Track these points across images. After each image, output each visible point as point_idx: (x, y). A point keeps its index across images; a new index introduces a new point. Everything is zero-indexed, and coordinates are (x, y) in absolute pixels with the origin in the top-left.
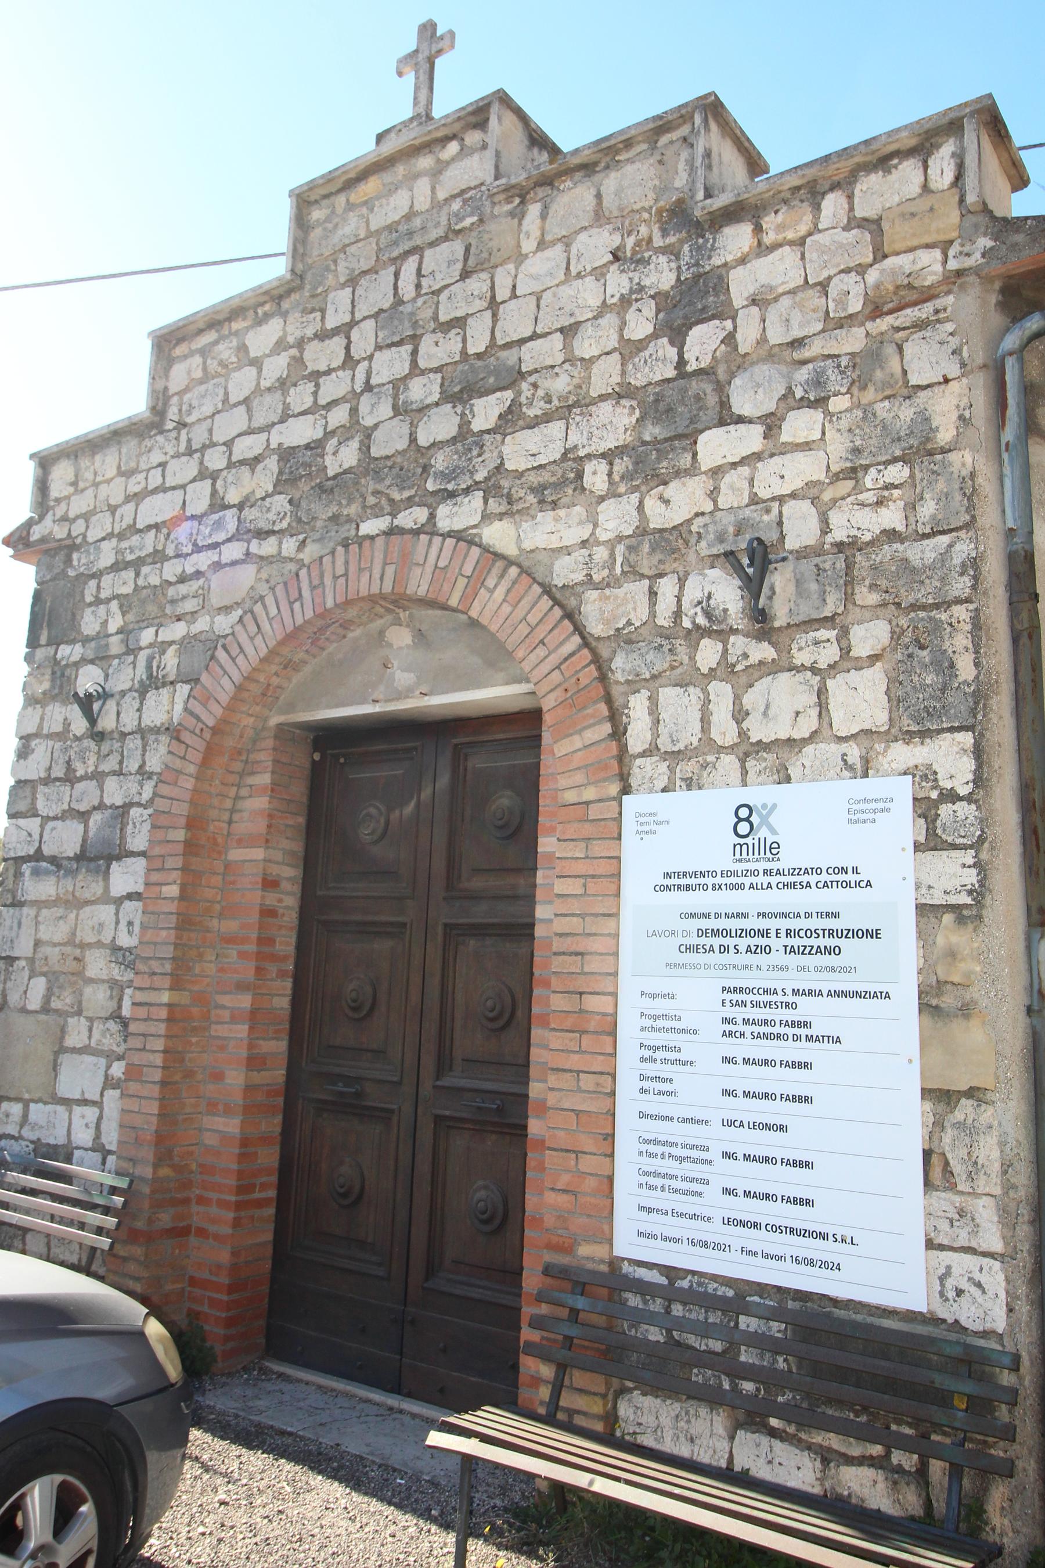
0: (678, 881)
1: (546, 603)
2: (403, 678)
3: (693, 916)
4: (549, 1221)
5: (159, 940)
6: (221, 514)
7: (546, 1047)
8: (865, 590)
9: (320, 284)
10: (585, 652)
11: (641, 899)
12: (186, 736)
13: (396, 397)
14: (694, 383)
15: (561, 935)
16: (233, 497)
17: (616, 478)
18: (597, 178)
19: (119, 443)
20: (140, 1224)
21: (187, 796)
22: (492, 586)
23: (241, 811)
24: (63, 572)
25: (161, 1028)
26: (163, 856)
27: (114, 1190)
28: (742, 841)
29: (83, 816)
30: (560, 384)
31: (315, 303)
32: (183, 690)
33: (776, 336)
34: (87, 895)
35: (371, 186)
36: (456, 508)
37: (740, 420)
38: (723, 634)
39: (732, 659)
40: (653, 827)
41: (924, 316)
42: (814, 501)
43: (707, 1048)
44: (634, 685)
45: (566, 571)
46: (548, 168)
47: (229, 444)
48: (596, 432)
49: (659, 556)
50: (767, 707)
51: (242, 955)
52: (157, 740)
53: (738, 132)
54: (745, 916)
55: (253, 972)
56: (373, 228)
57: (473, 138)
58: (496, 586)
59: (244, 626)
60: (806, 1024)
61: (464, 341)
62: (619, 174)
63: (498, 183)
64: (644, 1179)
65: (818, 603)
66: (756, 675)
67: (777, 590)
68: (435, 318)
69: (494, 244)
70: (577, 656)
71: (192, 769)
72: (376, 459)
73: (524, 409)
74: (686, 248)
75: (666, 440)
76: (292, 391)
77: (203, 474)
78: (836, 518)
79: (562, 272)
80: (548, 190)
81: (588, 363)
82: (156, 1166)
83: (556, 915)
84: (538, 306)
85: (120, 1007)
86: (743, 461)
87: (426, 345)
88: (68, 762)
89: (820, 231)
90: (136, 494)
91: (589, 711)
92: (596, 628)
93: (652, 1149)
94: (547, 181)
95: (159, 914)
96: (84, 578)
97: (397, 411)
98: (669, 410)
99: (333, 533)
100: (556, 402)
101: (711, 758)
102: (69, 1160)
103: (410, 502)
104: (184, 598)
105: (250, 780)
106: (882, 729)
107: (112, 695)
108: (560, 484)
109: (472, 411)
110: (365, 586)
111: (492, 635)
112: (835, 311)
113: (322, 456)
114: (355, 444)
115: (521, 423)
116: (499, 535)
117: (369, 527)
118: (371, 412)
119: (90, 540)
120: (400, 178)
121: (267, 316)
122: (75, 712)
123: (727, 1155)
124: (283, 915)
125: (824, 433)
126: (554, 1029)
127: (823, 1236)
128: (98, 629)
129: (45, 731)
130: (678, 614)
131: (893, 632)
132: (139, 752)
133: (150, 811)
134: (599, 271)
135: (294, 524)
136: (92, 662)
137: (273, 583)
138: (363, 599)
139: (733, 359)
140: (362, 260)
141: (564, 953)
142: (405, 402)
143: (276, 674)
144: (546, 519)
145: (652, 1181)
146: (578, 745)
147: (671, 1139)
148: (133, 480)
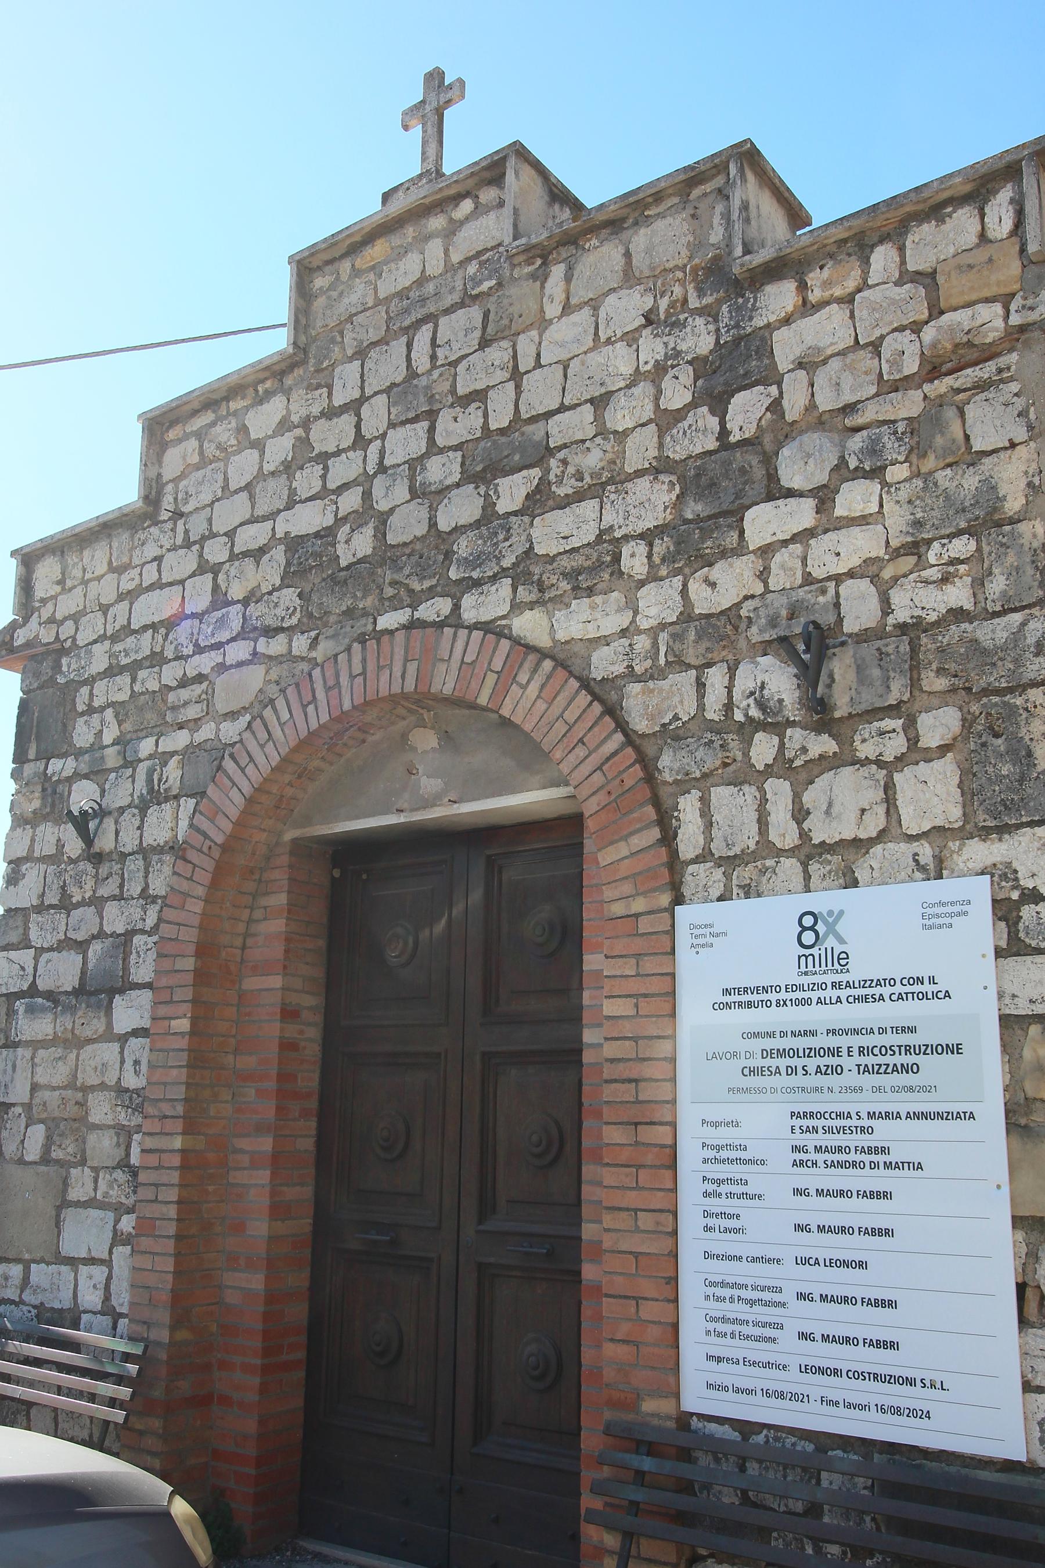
0: (739, 997)
1: (584, 698)
2: (429, 785)
3: (756, 1035)
4: (609, 1374)
5: (169, 1080)
6: (224, 610)
7: (599, 1184)
8: (932, 674)
9: (325, 357)
10: (629, 750)
11: (700, 1020)
12: (192, 855)
13: (412, 479)
14: (738, 455)
15: (612, 1061)
16: (237, 592)
17: (657, 559)
18: (625, 235)
19: (109, 536)
20: (158, 1393)
21: (196, 921)
22: (524, 682)
23: (254, 935)
24: (52, 680)
25: (175, 1177)
26: (171, 987)
27: (127, 1357)
28: (807, 952)
29: (82, 946)
30: (593, 460)
31: (321, 379)
32: (188, 804)
33: (826, 401)
34: (88, 1032)
35: (378, 250)
36: (483, 597)
37: (790, 493)
38: (778, 728)
39: (789, 754)
40: (710, 940)
41: (986, 376)
42: (874, 579)
43: (775, 1180)
44: (683, 786)
45: (605, 663)
46: (576, 228)
47: (231, 534)
48: (633, 511)
49: (705, 644)
50: (830, 805)
51: (260, 1093)
52: (160, 860)
53: (777, 181)
54: (813, 1033)
55: (273, 1112)
56: (382, 295)
57: (488, 195)
58: (528, 682)
59: (253, 733)
60: (884, 1150)
61: (486, 416)
62: (649, 231)
63: (517, 243)
64: (711, 1326)
65: (881, 690)
66: (815, 772)
67: (837, 677)
68: (453, 391)
69: (515, 310)
70: (620, 755)
71: (200, 891)
72: (393, 546)
73: (554, 488)
74: (725, 308)
75: (710, 517)
76: (298, 475)
77: (203, 568)
78: (898, 597)
79: (591, 337)
80: (572, 249)
81: (621, 436)
82: (173, 1328)
83: (606, 1039)
84: (565, 376)
85: (128, 1155)
86: (794, 538)
87: (444, 420)
88: (63, 887)
89: (870, 287)
90: (129, 592)
91: (634, 815)
92: (640, 725)
93: (720, 1292)
94: (572, 240)
95: (167, 1051)
96: (72, 686)
97: (414, 494)
98: (712, 484)
99: (348, 629)
100: (588, 479)
101: (770, 863)
102: (76, 1326)
103: (431, 593)
104: (186, 704)
105: (264, 901)
106: (956, 826)
107: (110, 813)
108: (596, 569)
109: (496, 491)
110: (384, 685)
111: (527, 735)
112: (890, 373)
113: (334, 545)
114: (369, 531)
115: (551, 503)
116: (530, 625)
117: (388, 621)
118: (387, 495)
119: (80, 643)
120: (410, 240)
121: (269, 394)
122: (69, 832)
123: (802, 1296)
124: (305, 1048)
125: (881, 506)
126: (608, 1164)
127: (910, 1382)
128: (91, 740)
129: (37, 854)
130: (729, 707)
131: (964, 720)
132: (141, 874)
133: (155, 938)
134: (630, 336)
135: (305, 620)
136: (86, 776)
137: (283, 684)
138: (383, 699)
139: (780, 429)
140: (371, 330)
141: (616, 1081)
142: (422, 484)
143: (290, 784)
144: (581, 606)
146: (625, 852)
147: (741, 1281)
148: (125, 577)
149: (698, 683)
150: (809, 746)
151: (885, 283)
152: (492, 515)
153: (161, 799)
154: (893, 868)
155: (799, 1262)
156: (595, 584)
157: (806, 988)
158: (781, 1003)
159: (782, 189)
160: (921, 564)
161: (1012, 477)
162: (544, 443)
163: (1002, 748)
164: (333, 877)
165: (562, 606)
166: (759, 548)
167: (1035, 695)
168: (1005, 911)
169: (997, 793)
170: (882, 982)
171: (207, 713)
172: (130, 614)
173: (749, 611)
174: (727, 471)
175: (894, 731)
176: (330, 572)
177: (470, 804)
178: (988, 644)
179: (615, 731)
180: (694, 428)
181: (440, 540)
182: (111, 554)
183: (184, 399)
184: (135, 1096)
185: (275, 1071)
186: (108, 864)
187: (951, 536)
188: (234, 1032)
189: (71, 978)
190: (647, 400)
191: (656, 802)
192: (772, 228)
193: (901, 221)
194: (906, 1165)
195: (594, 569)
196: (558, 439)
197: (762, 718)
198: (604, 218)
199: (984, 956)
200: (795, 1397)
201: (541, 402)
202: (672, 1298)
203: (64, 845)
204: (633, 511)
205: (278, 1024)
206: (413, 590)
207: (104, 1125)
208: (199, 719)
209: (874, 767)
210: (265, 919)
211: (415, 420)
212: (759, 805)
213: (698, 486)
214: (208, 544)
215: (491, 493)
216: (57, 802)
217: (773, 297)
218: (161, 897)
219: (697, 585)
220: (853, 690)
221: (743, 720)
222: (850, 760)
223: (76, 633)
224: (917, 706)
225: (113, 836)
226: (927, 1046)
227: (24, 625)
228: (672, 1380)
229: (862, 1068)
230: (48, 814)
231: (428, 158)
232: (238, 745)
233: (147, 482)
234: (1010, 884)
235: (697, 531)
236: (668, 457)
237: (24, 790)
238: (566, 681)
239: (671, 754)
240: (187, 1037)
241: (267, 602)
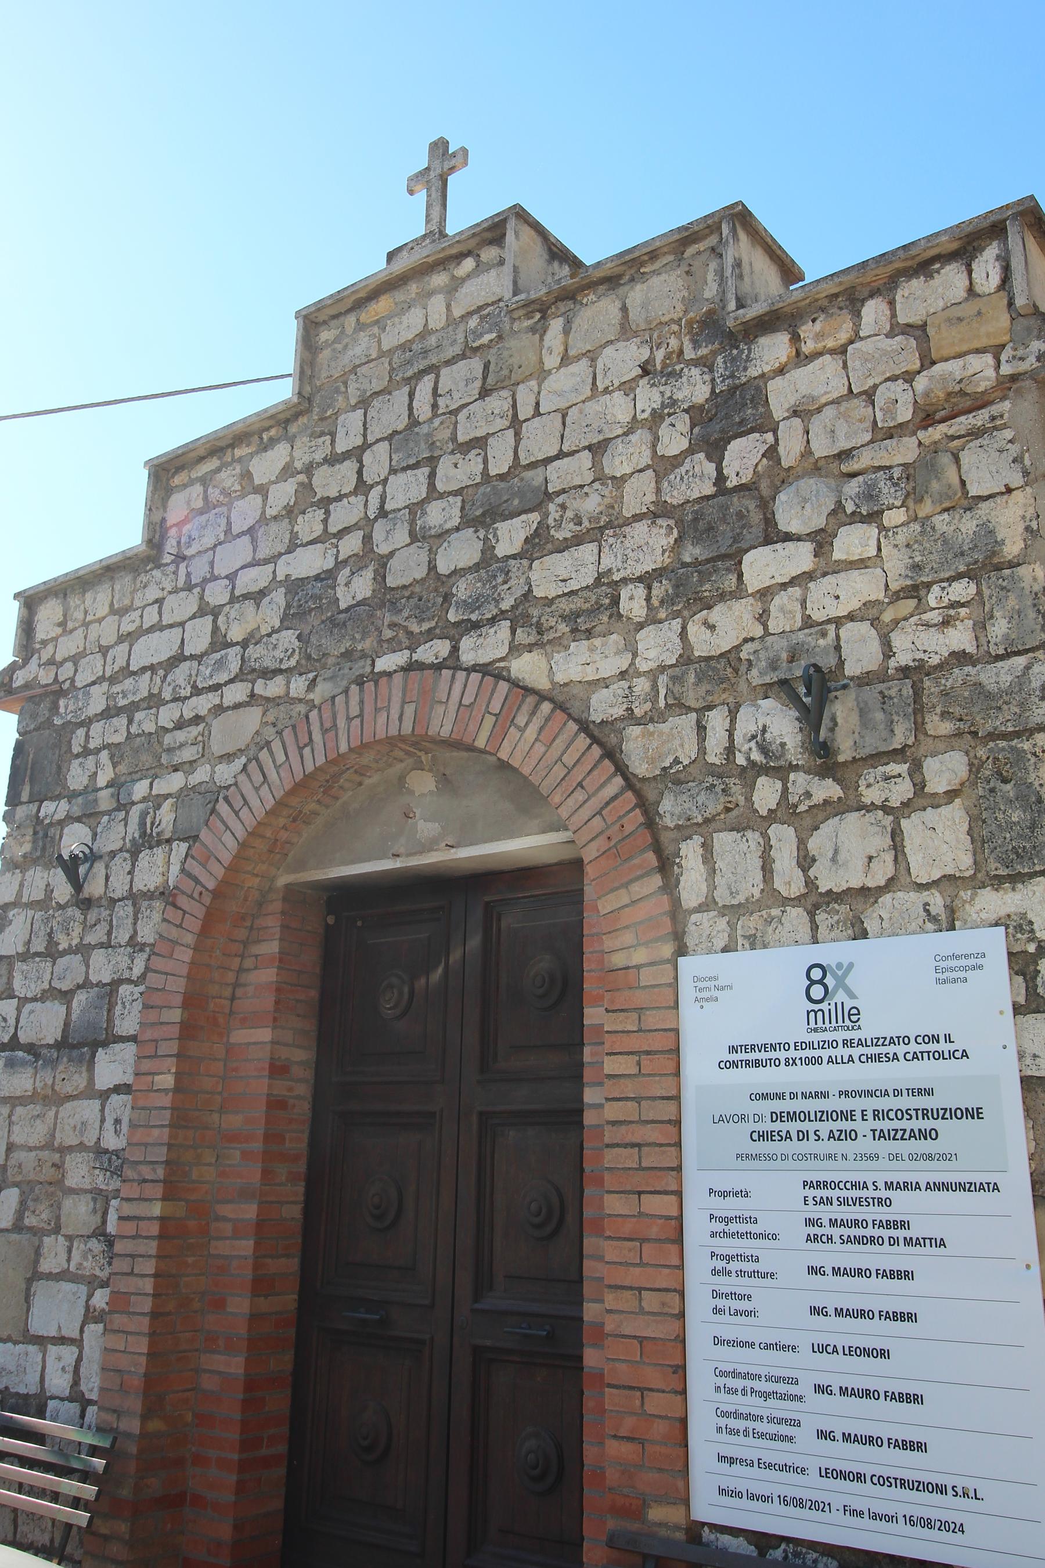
0: (745, 1056)
1: (583, 741)
2: (426, 829)
3: (765, 1096)
4: (612, 1476)
5: (150, 1140)
6: (223, 652)
7: (600, 1258)
8: (936, 718)
9: (329, 407)
10: (629, 794)
11: (703, 1073)
12: (183, 901)
13: (412, 522)
14: (735, 499)
15: (614, 1123)
16: (236, 634)
17: (655, 602)
18: (621, 291)
19: (112, 579)
20: (125, 1492)
21: (184, 971)
22: (522, 725)
23: (245, 985)
24: (49, 722)
25: (152, 1247)
26: (156, 1041)
27: (94, 1451)
28: (816, 1007)
29: (66, 996)
30: (591, 504)
31: (324, 427)
32: (180, 849)
33: (821, 448)
34: (68, 1089)
35: (383, 305)
36: (481, 640)
37: (788, 537)
38: (782, 772)
39: (793, 799)
40: (715, 993)
41: (980, 423)
42: (875, 622)
43: (789, 1256)
44: (685, 830)
45: (604, 706)
46: (572, 283)
47: (232, 577)
48: (631, 554)
49: (705, 687)
50: (836, 852)
51: (245, 1155)
52: (150, 907)
53: (769, 240)
54: (825, 1095)
55: (259, 1176)
56: (385, 347)
57: (489, 254)
58: (527, 724)
59: (249, 776)
60: (903, 1225)
61: (485, 462)
62: (645, 286)
63: (516, 298)
64: (723, 1422)
65: (885, 734)
66: (820, 817)
67: (839, 720)
68: (454, 438)
69: (515, 361)
70: (621, 799)
71: (189, 939)
72: (393, 589)
73: (552, 532)
74: (720, 359)
75: (708, 561)
76: (300, 519)
77: (204, 609)
78: (899, 641)
79: (589, 387)
80: (570, 304)
81: (619, 481)
82: (145, 1418)
83: (607, 1099)
84: (564, 424)
85: (104, 1222)
86: (793, 582)
87: (444, 467)
88: (50, 935)
89: (862, 339)
90: (129, 634)
91: (636, 861)
92: (640, 768)
93: (731, 1383)
94: (569, 296)
95: (150, 1109)
96: (70, 727)
97: (414, 537)
98: (710, 528)
99: (346, 671)
100: (586, 523)
101: (775, 912)
102: (41, 1414)
103: (430, 635)
104: (182, 745)
105: (256, 949)
106: (967, 874)
107: (101, 857)
108: (594, 611)
109: (495, 535)
110: (382, 727)
111: (525, 778)
112: (884, 421)
113: (334, 588)
114: (369, 574)
115: (549, 546)
116: (528, 667)
117: (386, 662)
118: (387, 539)
119: (79, 684)
120: (413, 296)
121: (273, 442)
122: (59, 878)
123: (820, 1389)
124: (294, 1106)
125: (879, 549)
126: (609, 1238)
127: (941, 1489)
128: (86, 782)
129: (24, 900)
130: (730, 750)
131: (971, 765)
132: (130, 920)
133: (142, 988)
134: (627, 386)
135: (303, 662)
136: (78, 820)
137: (280, 726)
138: (380, 741)
139: (776, 474)
140: (374, 381)
141: (618, 1145)
142: (423, 528)
143: (285, 828)
144: (580, 649)
145: (731, 1383)
146: (626, 900)
147: (754, 1370)
148: (126, 619)
149: (698, 726)
150: (813, 791)
151: (877, 335)
152: (491, 559)
153: (153, 843)
154: (903, 919)
155: (816, 1349)
156: (594, 627)
157: (816, 1046)
158: (790, 1062)
159: (774, 247)
160: (922, 607)
161: (1009, 521)
162: (543, 488)
163: (1011, 794)
164: (327, 925)
165: (561, 648)
166: (758, 591)
167: (1043, 739)
168: (1022, 965)
169: (1008, 840)
170: (896, 1040)
171: (203, 756)
172: (129, 655)
173: (749, 654)
174: (724, 515)
175: (900, 775)
176: (329, 614)
177: (468, 848)
178: (992, 688)
179: (614, 775)
180: (691, 474)
181: (440, 584)
182: (113, 597)
183: (190, 446)
184: (114, 1157)
185: (262, 1132)
186: (96, 910)
187: (951, 580)
188: (220, 1089)
189: (53, 1030)
190: (644, 447)
191: (657, 848)
192: (766, 286)
193: (890, 277)
194: (928, 1241)
195: (593, 611)
196: (557, 485)
197: (764, 761)
198: (602, 275)
199: (1001, 1013)
200: (816, 1506)
201: (540, 449)
202: (680, 1388)
203: (52, 891)
204: (631, 554)
205: (266, 1080)
206: (412, 633)
207: (81, 1189)
208: (195, 761)
209: (880, 813)
210: (256, 968)
211: (416, 466)
212: (764, 852)
213: (696, 530)
214: (209, 587)
215: (490, 537)
216: (48, 846)
217: (766, 349)
218: (149, 945)
219: (696, 628)
220: (856, 734)
221: (745, 763)
222: (855, 805)
223: (75, 674)
224: (922, 750)
225: (102, 881)
226: (946, 1110)
227: (24, 666)
228: (680, 1484)
229: (877, 1133)
230: (38, 858)
231: (432, 220)
232: (233, 788)
233: (151, 527)
234: (1026, 936)
235: (695, 574)
236: (666, 502)
237: (15, 834)
238: (565, 724)
239: (672, 798)
240: (171, 1094)
241: (266, 644)
